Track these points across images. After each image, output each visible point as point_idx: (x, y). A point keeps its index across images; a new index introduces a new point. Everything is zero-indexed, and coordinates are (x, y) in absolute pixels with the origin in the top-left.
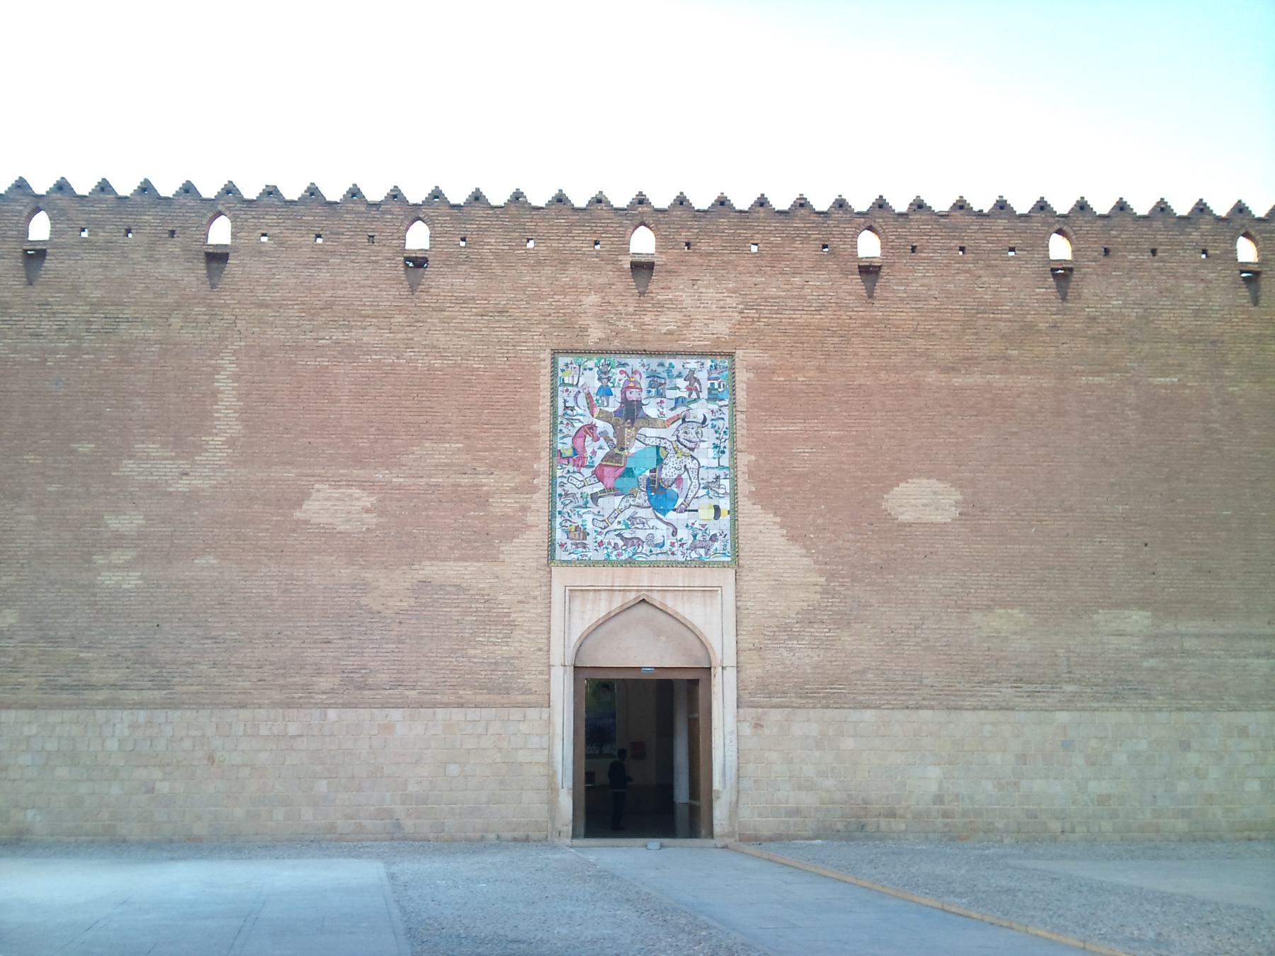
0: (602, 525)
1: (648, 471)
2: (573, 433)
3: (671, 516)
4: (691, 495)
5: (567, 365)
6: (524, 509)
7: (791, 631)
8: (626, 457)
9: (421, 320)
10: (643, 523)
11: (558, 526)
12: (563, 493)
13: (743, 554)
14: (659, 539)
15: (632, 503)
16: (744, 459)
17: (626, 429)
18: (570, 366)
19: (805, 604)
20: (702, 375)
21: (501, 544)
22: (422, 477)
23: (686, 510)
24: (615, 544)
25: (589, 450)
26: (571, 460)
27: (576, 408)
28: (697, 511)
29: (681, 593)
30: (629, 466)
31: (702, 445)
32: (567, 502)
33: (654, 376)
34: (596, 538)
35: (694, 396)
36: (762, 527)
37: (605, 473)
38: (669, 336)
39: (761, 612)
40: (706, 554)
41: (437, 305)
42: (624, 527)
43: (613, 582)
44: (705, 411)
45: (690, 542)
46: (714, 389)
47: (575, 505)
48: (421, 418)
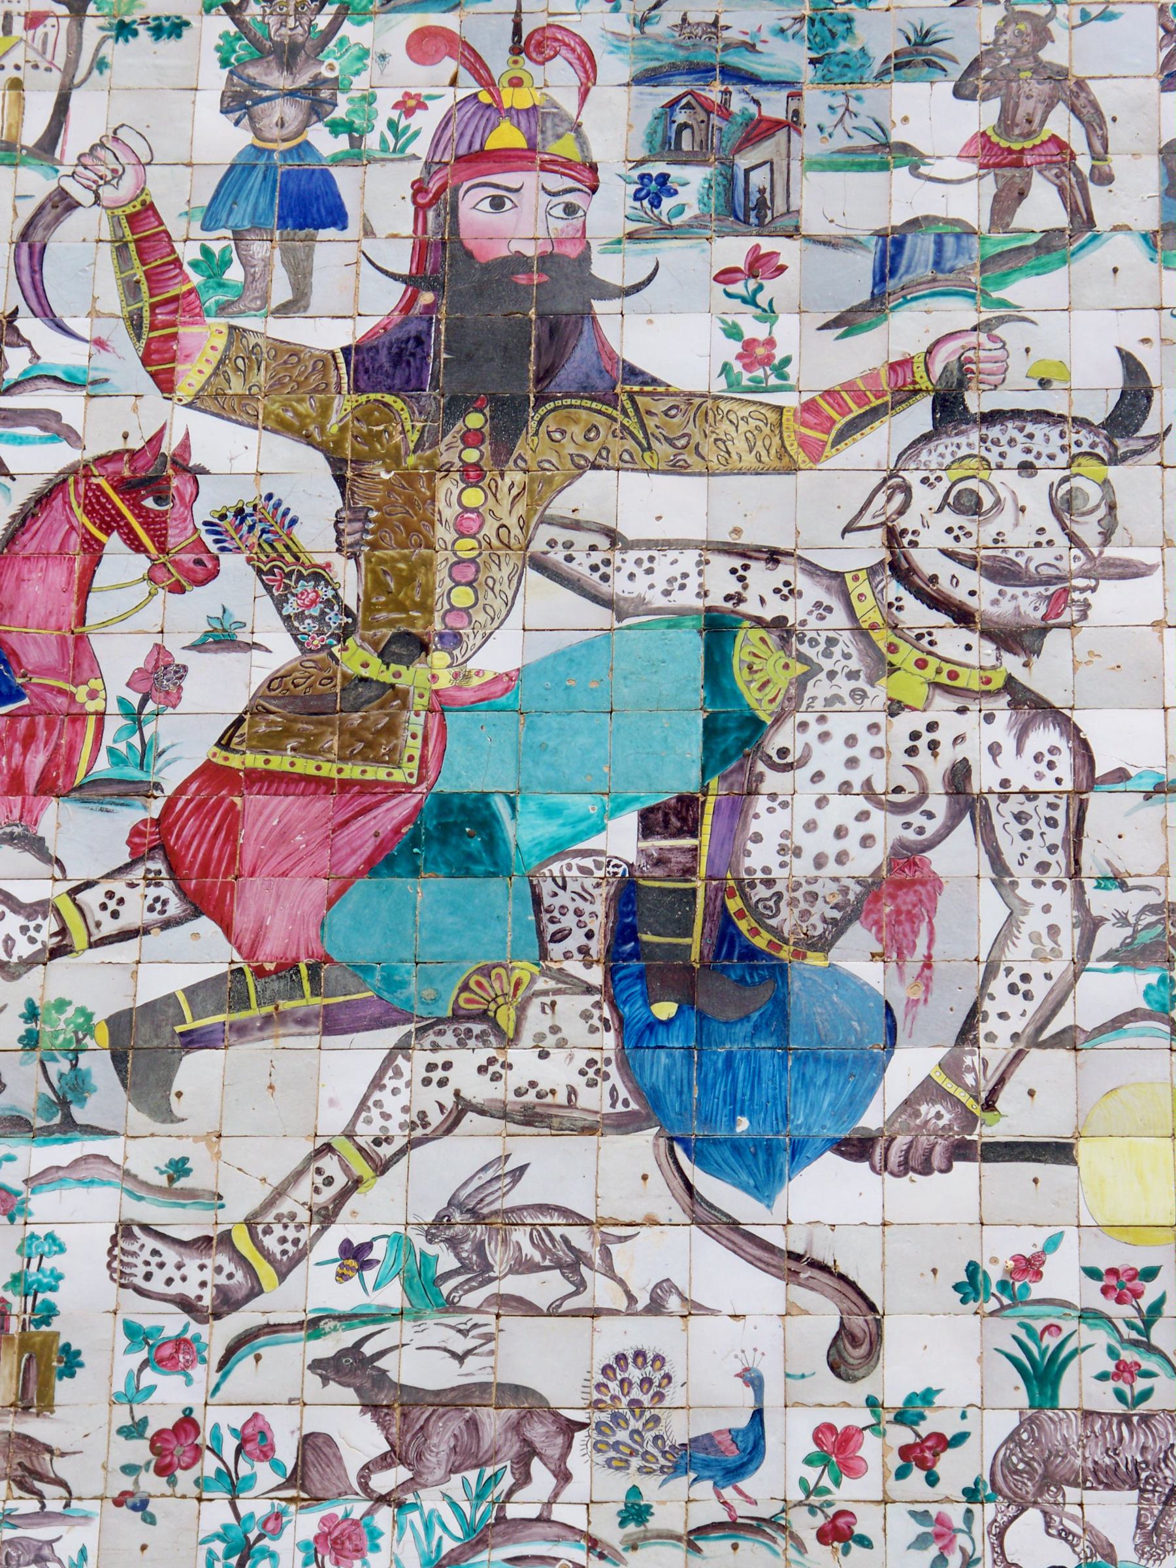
1: (629, 821)
8: (440, 705)
15: (479, 1090)
17: (448, 489)
23: (961, 1151)
27: (28, 325)
33: (703, 71)
34: (135, 1394)
37: (250, 839)
42: (393, 1296)
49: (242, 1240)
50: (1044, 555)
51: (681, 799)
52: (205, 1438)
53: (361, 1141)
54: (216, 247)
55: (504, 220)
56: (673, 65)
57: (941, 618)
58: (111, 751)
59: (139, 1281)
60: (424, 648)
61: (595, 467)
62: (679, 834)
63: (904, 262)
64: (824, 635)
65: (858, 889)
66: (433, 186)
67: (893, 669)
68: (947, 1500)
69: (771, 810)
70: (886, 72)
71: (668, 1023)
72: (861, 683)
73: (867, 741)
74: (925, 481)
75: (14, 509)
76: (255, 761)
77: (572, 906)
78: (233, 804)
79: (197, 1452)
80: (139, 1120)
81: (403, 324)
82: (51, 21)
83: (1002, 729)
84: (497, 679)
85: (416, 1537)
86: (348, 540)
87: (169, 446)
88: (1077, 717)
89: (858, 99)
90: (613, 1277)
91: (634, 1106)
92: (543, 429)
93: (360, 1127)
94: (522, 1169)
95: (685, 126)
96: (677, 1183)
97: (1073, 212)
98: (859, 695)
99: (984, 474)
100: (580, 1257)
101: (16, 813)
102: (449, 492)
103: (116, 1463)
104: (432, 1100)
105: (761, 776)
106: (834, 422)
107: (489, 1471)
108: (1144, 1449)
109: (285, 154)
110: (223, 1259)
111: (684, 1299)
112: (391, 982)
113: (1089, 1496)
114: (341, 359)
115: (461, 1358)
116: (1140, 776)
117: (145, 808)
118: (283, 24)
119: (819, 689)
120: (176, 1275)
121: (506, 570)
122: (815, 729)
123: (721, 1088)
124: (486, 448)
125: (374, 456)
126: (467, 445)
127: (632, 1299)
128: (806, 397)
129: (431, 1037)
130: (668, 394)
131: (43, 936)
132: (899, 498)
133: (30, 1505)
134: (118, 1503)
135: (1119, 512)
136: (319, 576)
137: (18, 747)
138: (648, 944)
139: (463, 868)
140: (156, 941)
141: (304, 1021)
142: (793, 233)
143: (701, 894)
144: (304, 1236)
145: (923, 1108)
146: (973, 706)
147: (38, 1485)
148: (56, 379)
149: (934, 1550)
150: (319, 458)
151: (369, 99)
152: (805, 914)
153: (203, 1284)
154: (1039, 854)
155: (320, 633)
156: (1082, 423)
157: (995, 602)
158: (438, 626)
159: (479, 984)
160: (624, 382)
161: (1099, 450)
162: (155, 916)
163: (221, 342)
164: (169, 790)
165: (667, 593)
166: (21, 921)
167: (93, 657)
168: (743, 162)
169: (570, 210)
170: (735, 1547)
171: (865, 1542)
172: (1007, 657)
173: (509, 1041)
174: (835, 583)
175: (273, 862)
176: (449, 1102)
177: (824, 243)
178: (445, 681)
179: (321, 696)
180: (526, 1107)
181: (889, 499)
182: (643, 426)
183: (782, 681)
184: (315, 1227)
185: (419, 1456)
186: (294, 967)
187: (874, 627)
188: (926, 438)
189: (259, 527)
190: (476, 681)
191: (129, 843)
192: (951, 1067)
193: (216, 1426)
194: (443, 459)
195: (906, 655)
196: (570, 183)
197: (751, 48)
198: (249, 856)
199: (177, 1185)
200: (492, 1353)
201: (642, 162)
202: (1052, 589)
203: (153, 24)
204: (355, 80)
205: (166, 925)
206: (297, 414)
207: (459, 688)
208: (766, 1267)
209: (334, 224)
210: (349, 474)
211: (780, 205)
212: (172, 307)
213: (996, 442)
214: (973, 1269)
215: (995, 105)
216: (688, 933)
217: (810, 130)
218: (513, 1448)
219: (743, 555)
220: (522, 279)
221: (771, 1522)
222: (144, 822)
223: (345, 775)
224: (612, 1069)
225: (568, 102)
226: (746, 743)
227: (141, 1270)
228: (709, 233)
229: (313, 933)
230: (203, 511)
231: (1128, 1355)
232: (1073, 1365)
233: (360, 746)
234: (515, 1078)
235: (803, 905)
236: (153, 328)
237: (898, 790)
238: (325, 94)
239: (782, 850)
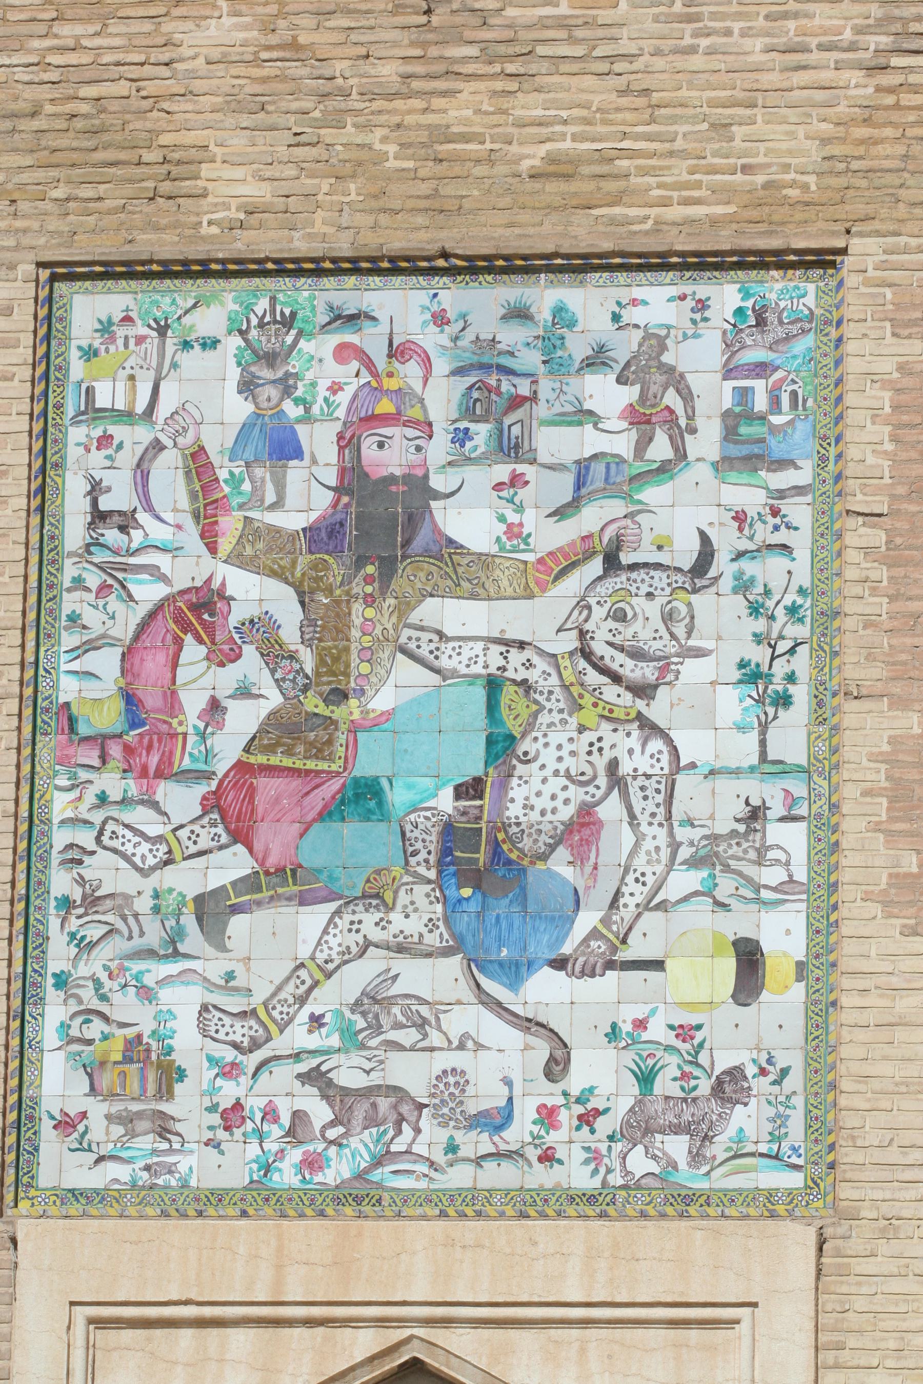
0: (240, 1032)
4: (634, 895)
5: (106, 328)
8: (354, 729)
10: (422, 1024)
11: (50, 1037)
12: (77, 894)
13: (858, 1157)
15: (376, 935)
17: (357, 607)
18: (121, 332)
23: (610, 965)
24: (298, 1116)
26: (115, 750)
27: (142, 517)
28: (658, 965)
29: (575, 1333)
30: (364, 767)
32: (94, 932)
33: (485, 367)
34: (213, 1090)
38: (552, 187)
40: (696, 1158)
42: (335, 1041)
43: (279, 1282)
44: (706, 517)
45: (624, 1105)
46: (752, 417)
50: (657, 645)
51: (474, 779)
52: (246, 1113)
53: (318, 961)
54: (237, 471)
55: (385, 453)
56: (472, 365)
57: (606, 680)
58: (191, 754)
59: (213, 1034)
60: (346, 696)
61: (432, 595)
62: (474, 798)
63: (590, 478)
64: (547, 689)
65: (562, 827)
66: (348, 436)
67: (581, 707)
68: (599, 1141)
69: (519, 785)
70: (582, 369)
71: (468, 899)
72: (565, 716)
73: (568, 747)
74: (598, 603)
75: (138, 620)
76: (262, 759)
77: (420, 837)
78: (252, 783)
79: (243, 1118)
80: (210, 951)
81: (333, 514)
82: (149, 340)
83: (634, 742)
84: (383, 714)
85: (348, 1161)
86: (307, 637)
87: (216, 584)
88: (672, 734)
89: (567, 384)
90: (442, 1031)
91: (451, 943)
92: (405, 574)
93: (318, 954)
94: (397, 976)
95: (477, 400)
96: (472, 983)
97: (676, 450)
98: (564, 722)
99: (628, 599)
100: (425, 1021)
101: (145, 788)
102: (357, 610)
103: (204, 1126)
105: (514, 767)
106: (553, 570)
107: (382, 1128)
108: (693, 1115)
109: (271, 416)
110: (252, 1023)
111: (475, 1043)
113: (666, 1138)
114: (302, 535)
115: (368, 1072)
116: (702, 766)
117: (209, 785)
118: (269, 341)
120: (231, 1030)
121: (387, 653)
122: (542, 741)
123: (493, 933)
124: (376, 585)
125: (319, 588)
126: (367, 583)
127: (450, 1042)
128: (539, 555)
129: (351, 907)
130: (469, 554)
131: (160, 854)
132: (585, 612)
133: (165, 1146)
134: (206, 1144)
135: (696, 620)
136: (292, 657)
137: (144, 753)
138: (458, 857)
139: (367, 817)
140: (216, 858)
141: (289, 899)
142: (533, 462)
143: (484, 831)
144: (291, 1010)
145: (592, 943)
146: (621, 728)
147: (168, 1136)
148: (156, 547)
149: (593, 1166)
150: (291, 591)
151: (314, 385)
152: (536, 841)
153: (244, 1035)
154: (651, 808)
155: (294, 689)
156: (678, 570)
157: (633, 671)
158: (353, 685)
159: (375, 879)
160: (447, 547)
161: (687, 586)
162: (215, 843)
163: (240, 526)
164: (220, 775)
165: (468, 666)
166: (149, 846)
167: (180, 703)
168: (507, 421)
169: (419, 449)
170: (499, 1165)
171: (560, 1162)
172: (638, 701)
173: (390, 908)
174: (552, 660)
175: (272, 815)
176: (361, 941)
177: (549, 468)
178: (356, 716)
179: (295, 723)
180: (399, 944)
181: (580, 613)
182: (456, 573)
183: (525, 714)
184: (297, 1006)
185: (349, 1121)
186: (283, 870)
187: (572, 684)
188: (599, 579)
189: (262, 630)
190: (372, 715)
191: (201, 804)
192: (606, 921)
193: (252, 1107)
194: (354, 592)
195: (588, 700)
196: (419, 434)
197: (512, 354)
198: (260, 811)
199: (229, 985)
200: (383, 1070)
201: (454, 421)
202: (661, 663)
203: (201, 341)
204: (307, 373)
205: (221, 848)
206: (280, 566)
207: (364, 719)
208: (515, 1026)
209: (297, 458)
210: (307, 600)
211: (526, 446)
212: (214, 506)
213: (635, 581)
214: (614, 1026)
215: (637, 388)
216: (478, 852)
217: (542, 403)
218: (394, 1117)
219: (507, 645)
220: (394, 489)
221: (515, 1152)
222: (208, 793)
223: (307, 767)
224: (441, 924)
225: (417, 386)
226: (507, 748)
227: (214, 1028)
228: (489, 462)
229: (293, 852)
230: (233, 621)
231: (687, 1068)
232: (661, 1073)
233: (315, 751)
234: (393, 929)
235: (535, 836)
236: (205, 518)
237: (583, 774)
238: (291, 382)
239: (525, 807)
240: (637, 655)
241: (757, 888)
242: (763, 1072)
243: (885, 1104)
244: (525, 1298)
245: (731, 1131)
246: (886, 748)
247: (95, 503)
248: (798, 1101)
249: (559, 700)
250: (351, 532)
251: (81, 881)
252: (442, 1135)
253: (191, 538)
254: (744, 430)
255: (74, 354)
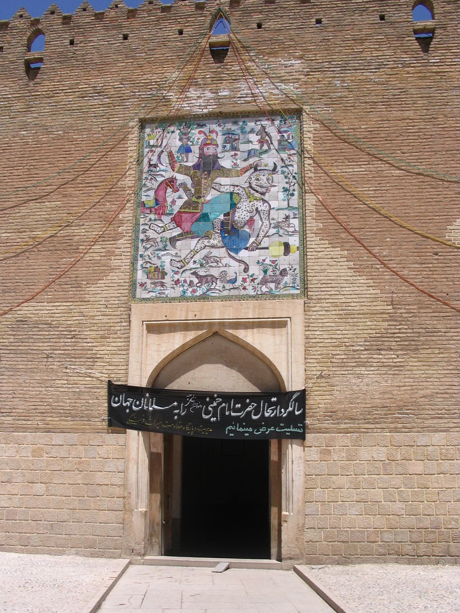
0: (179, 265)
1: (222, 215)
2: (156, 185)
3: (243, 254)
4: (262, 234)
6: (110, 254)
7: (359, 358)
8: (203, 203)
9: (34, 106)
10: (217, 262)
11: (139, 267)
13: (312, 286)
14: (231, 275)
15: (207, 244)
16: (311, 200)
17: (203, 181)
19: (374, 332)
20: (272, 131)
21: (88, 286)
22: (25, 232)
23: (257, 249)
24: (191, 282)
25: (169, 200)
26: (153, 210)
27: (159, 165)
28: (267, 248)
31: (272, 189)
32: (148, 246)
33: (229, 134)
34: (173, 277)
35: (265, 147)
36: (330, 260)
39: (329, 341)
40: (276, 288)
41: (48, 92)
42: (199, 266)
43: (187, 315)
44: (275, 160)
45: (261, 277)
47: (155, 248)
48: (28, 182)
49: (183, 261)
50: (266, 185)
73: (247, 205)
76: (183, 210)
80: (172, 248)
83: (261, 204)
87: (174, 177)
100: (218, 261)
104: (202, 245)
112: (198, 233)
119: (242, 200)
136: (190, 190)
151: (194, 138)
230: (177, 184)
240: (261, 187)
241: (288, 232)
242: (290, 269)
243: (317, 274)
244: (240, 317)
245: (284, 282)
246: (315, 203)
247: (150, 163)
248: (298, 275)
249: (245, 197)
250: (202, 166)
251: (146, 236)
252: (222, 285)
253: (169, 169)
254: (282, 143)
255: (146, 135)
